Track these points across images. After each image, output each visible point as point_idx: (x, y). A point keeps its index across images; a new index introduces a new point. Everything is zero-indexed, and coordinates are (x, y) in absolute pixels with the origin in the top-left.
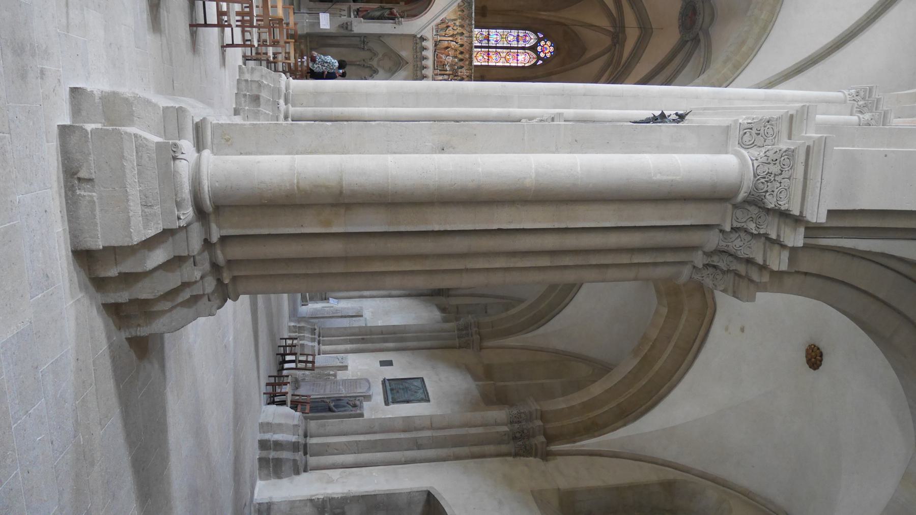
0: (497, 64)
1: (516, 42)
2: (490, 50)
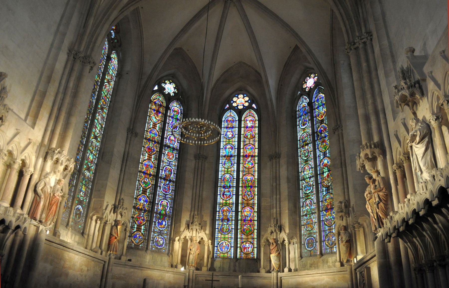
0: (257, 147)
1: (234, 130)
2: (242, 154)
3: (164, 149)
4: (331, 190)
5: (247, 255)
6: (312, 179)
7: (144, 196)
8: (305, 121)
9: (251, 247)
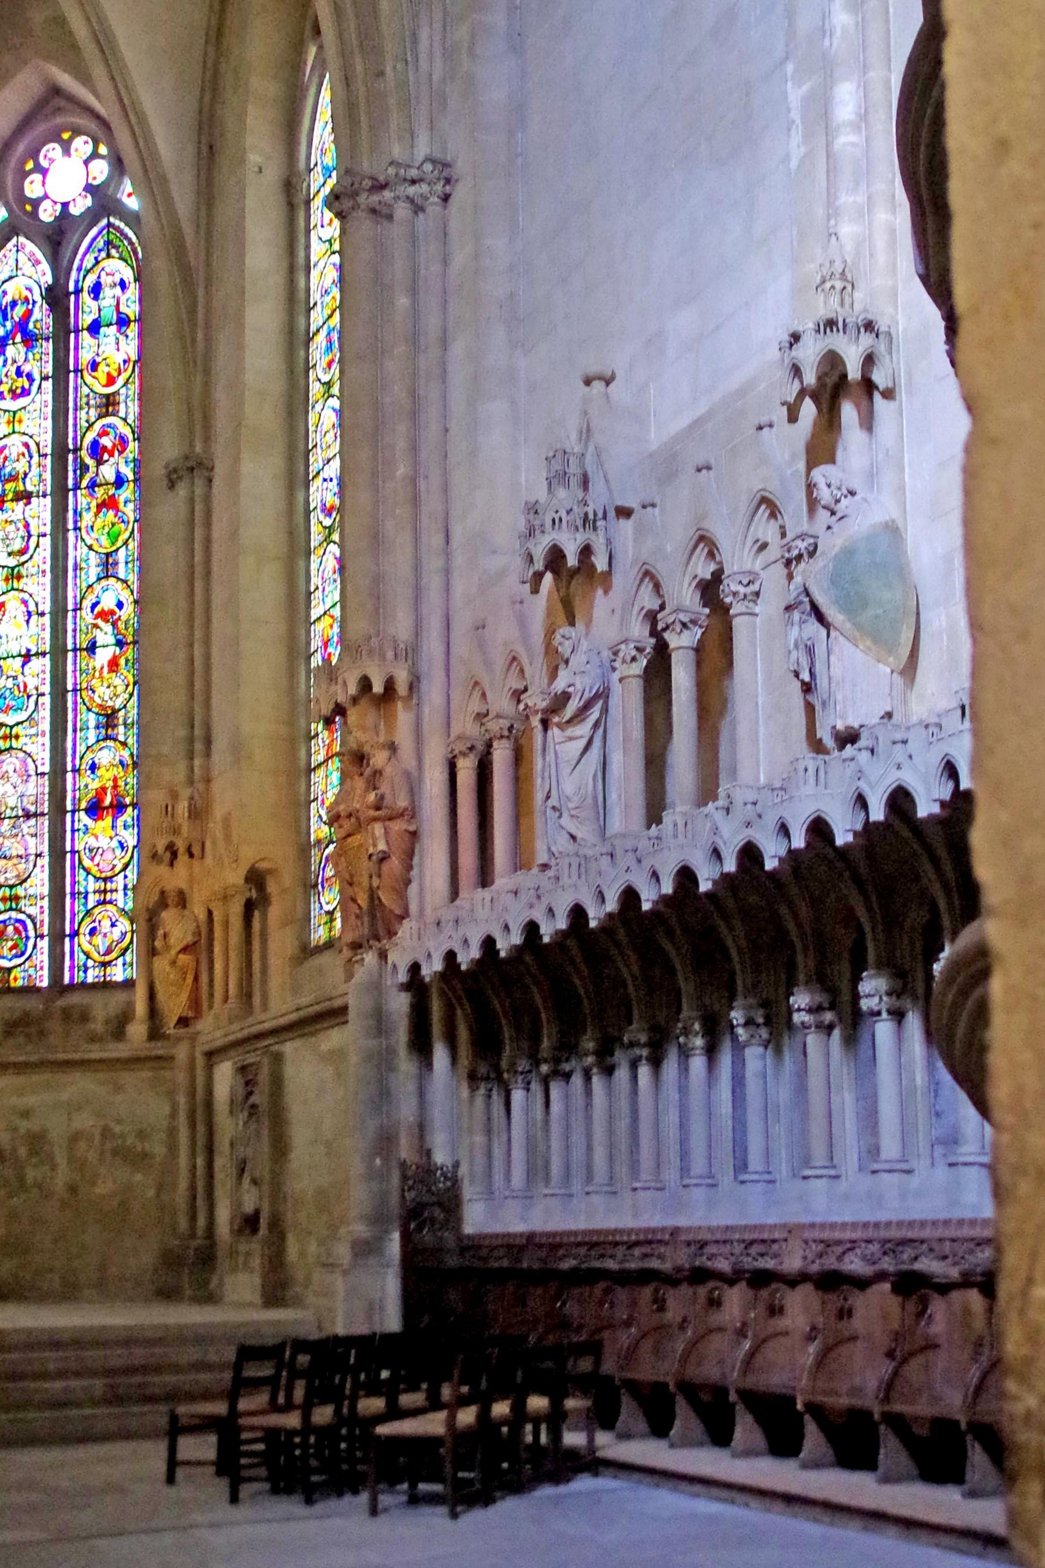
4: (121, 729)
6: (36, 664)
8: (19, 373)
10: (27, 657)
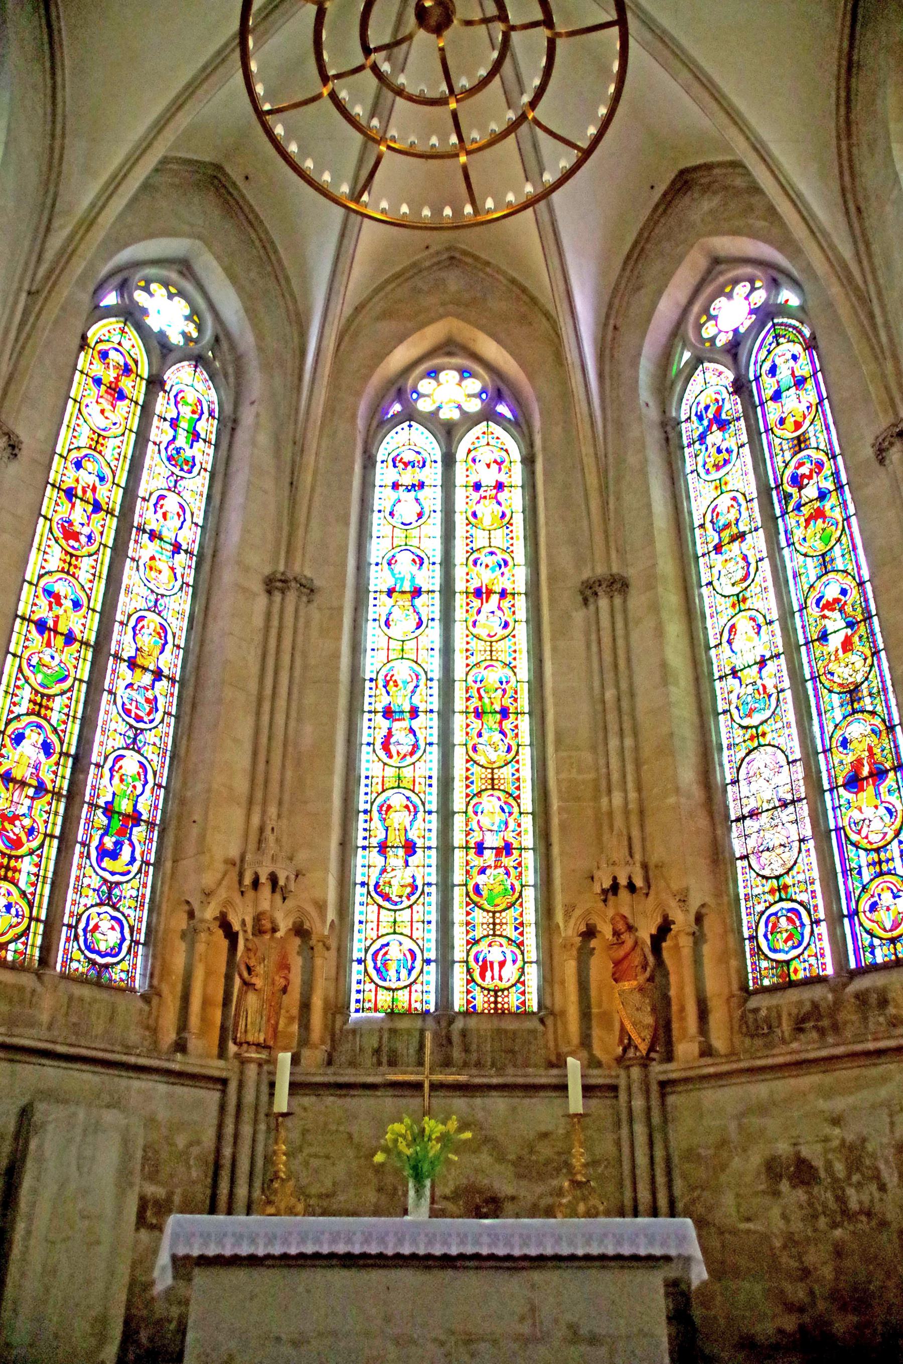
3: (136, 542)
4: (868, 700)
5: (496, 996)
6: (771, 666)
7: (39, 726)
8: (719, 451)
9: (514, 962)
10: (762, 663)
